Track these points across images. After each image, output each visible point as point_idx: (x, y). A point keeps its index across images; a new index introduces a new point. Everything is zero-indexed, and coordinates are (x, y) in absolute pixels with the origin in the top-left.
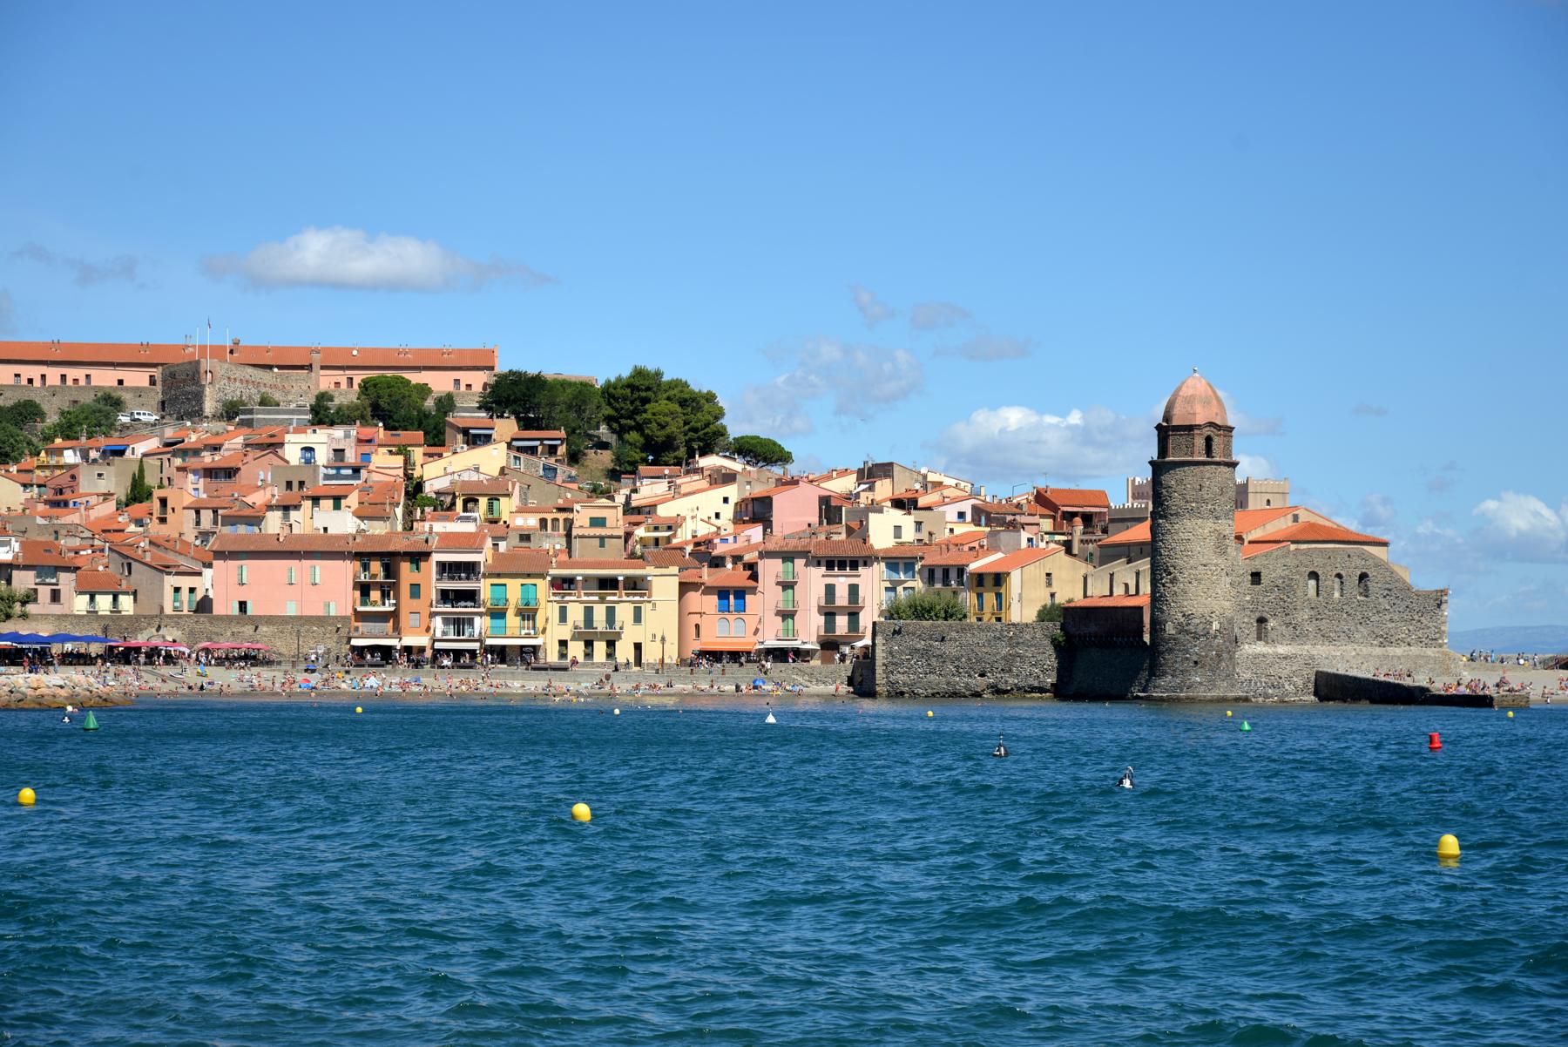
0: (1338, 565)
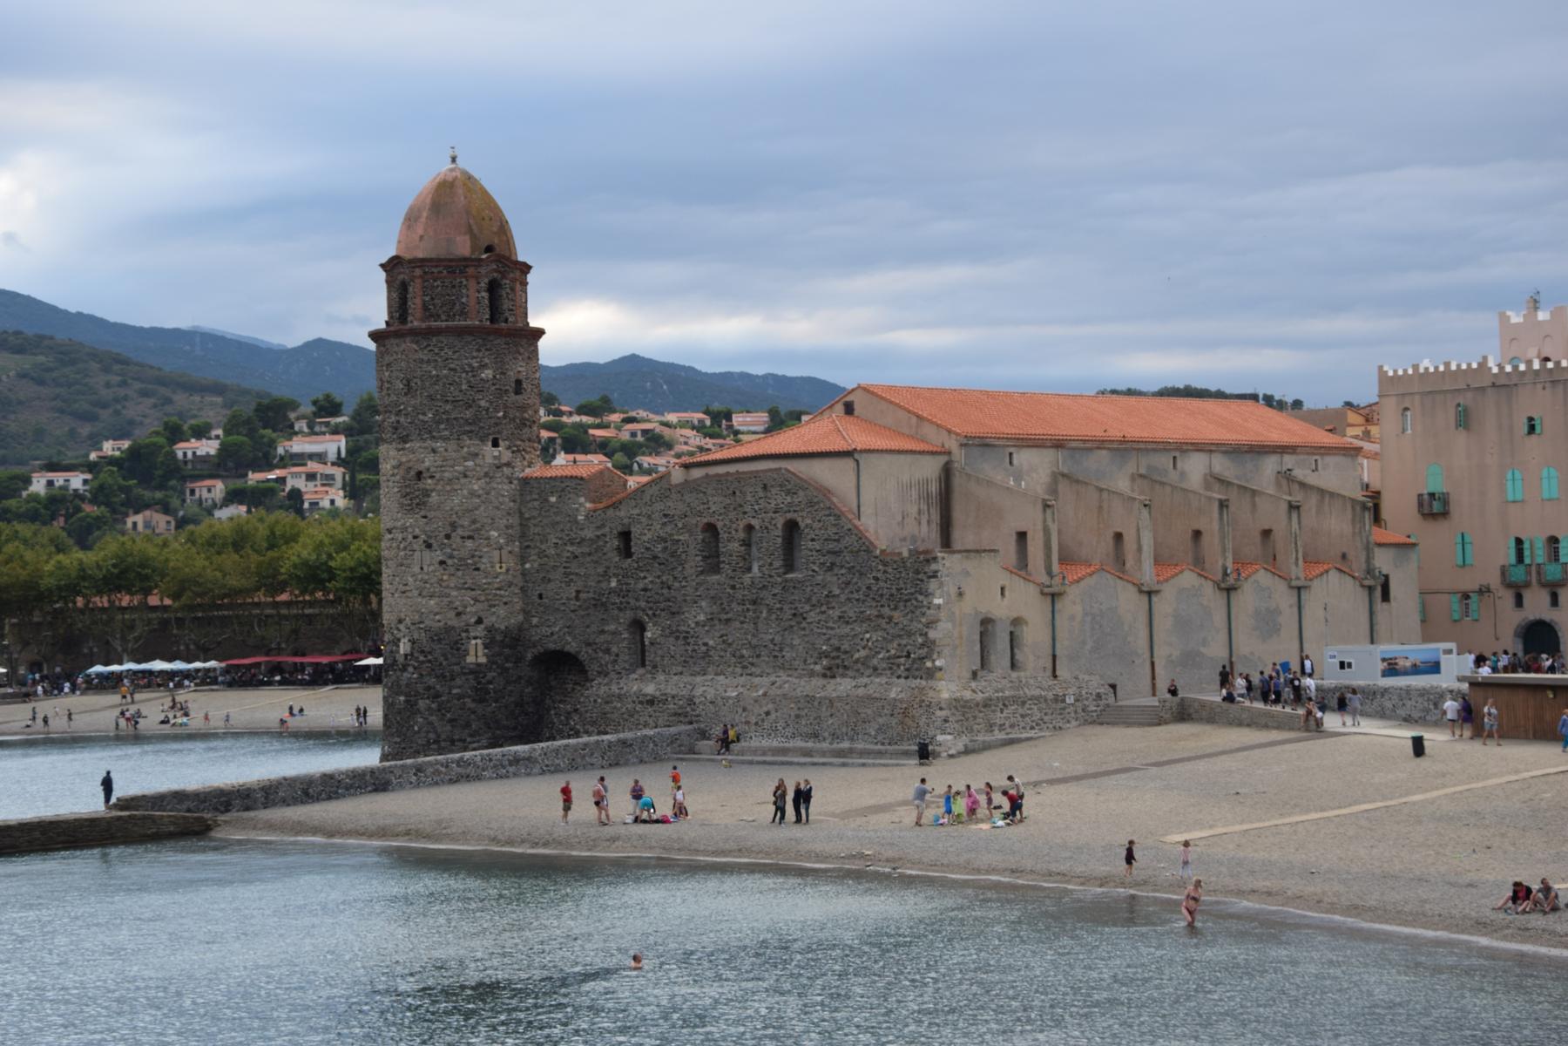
0: (748, 508)
